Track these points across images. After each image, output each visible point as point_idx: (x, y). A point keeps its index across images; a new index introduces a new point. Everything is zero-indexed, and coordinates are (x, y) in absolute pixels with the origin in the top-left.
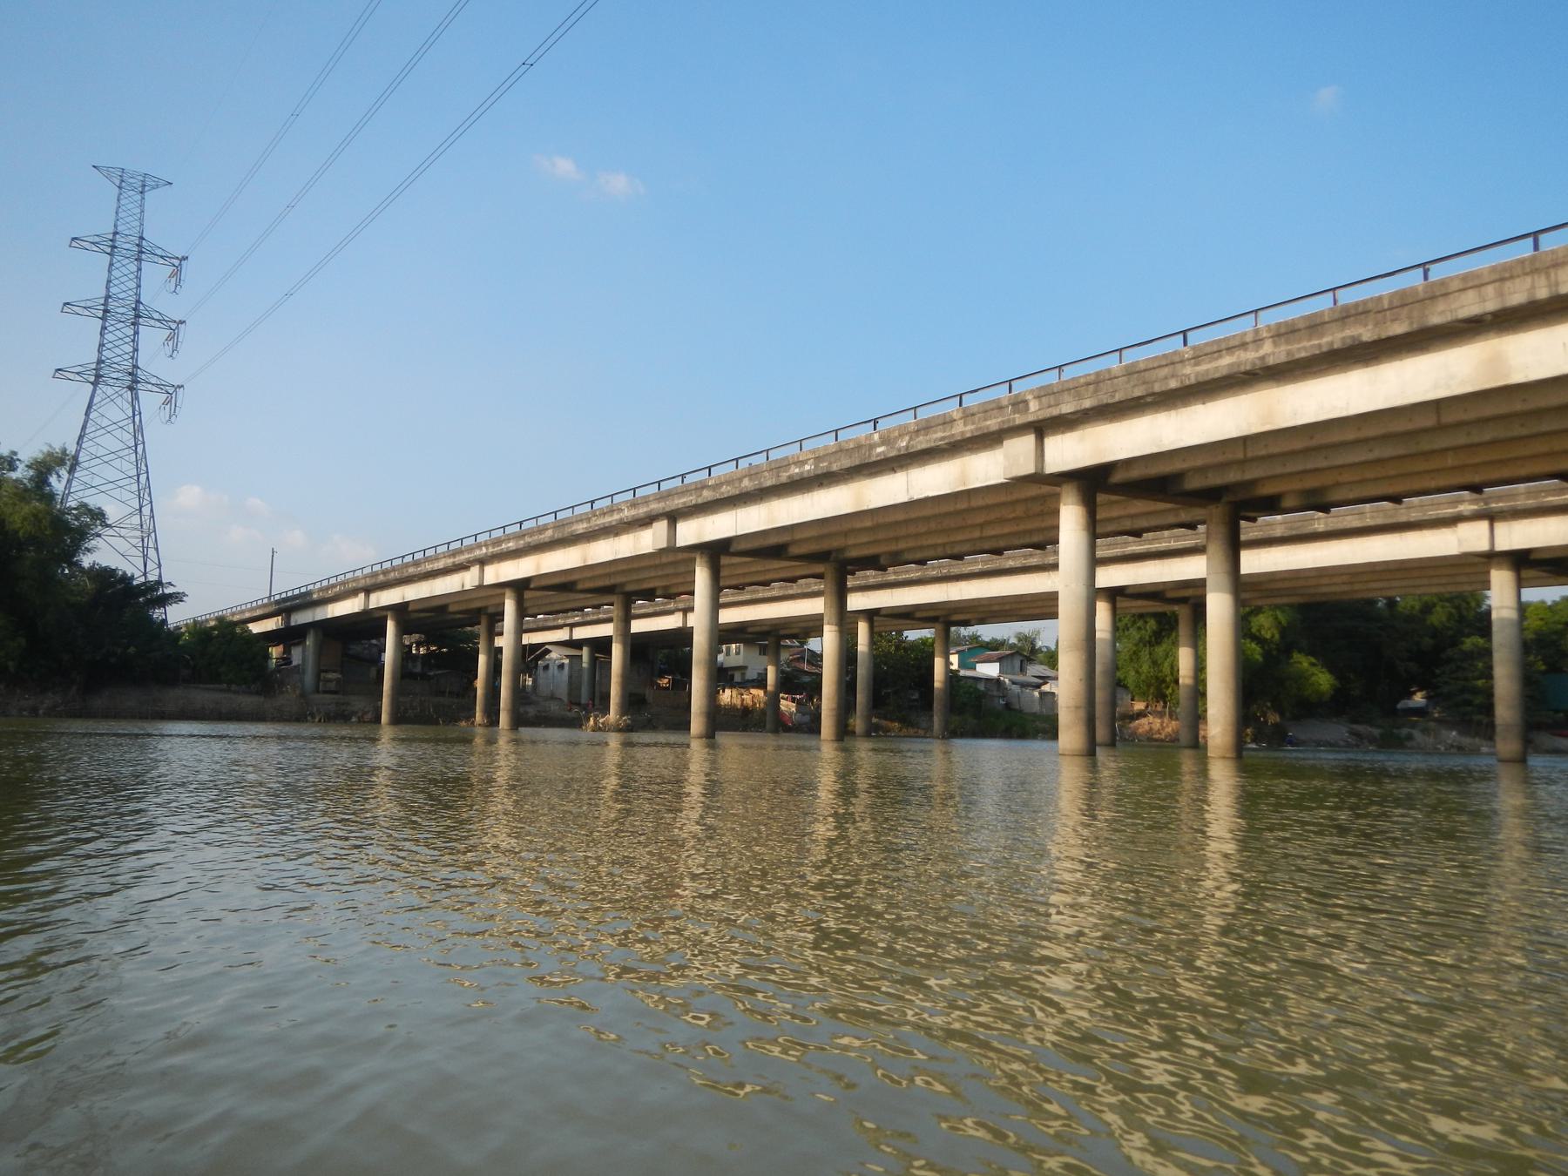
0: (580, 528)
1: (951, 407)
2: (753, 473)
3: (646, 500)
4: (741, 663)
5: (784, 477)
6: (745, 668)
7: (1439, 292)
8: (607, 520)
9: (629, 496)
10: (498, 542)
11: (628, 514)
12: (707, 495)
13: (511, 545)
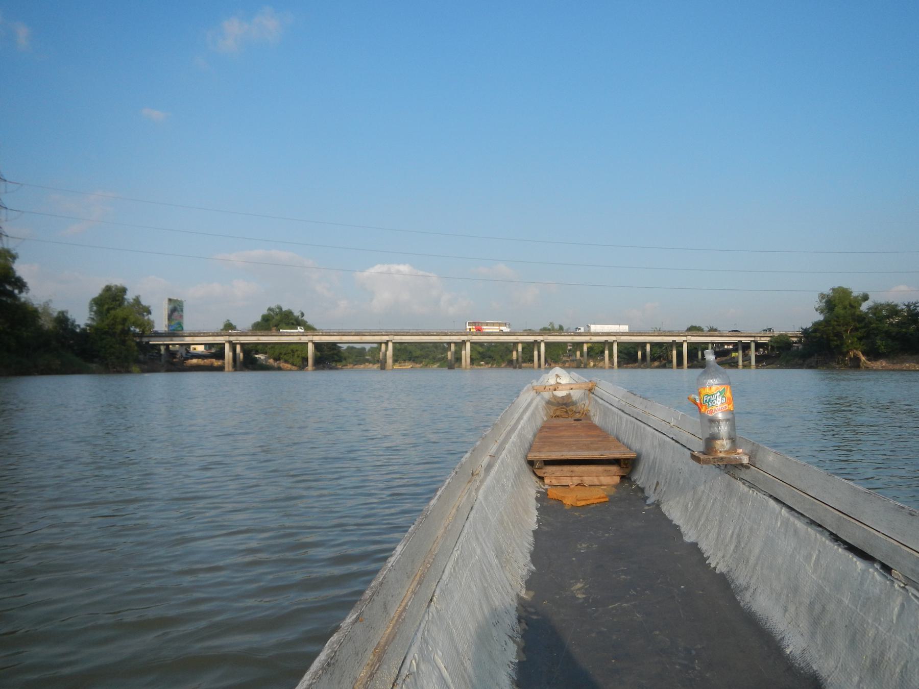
0: (366, 334)
1: (461, 331)
2: (421, 332)
3: (391, 332)
4: (178, 349)
5: (430, 334)
6: (178, 351)
7: (516, 332)
8: (377, 334)
9: (385, 331)
10: (329, 332)
11: (384, 333)
12: (409, 334)
13: (335, 334)
